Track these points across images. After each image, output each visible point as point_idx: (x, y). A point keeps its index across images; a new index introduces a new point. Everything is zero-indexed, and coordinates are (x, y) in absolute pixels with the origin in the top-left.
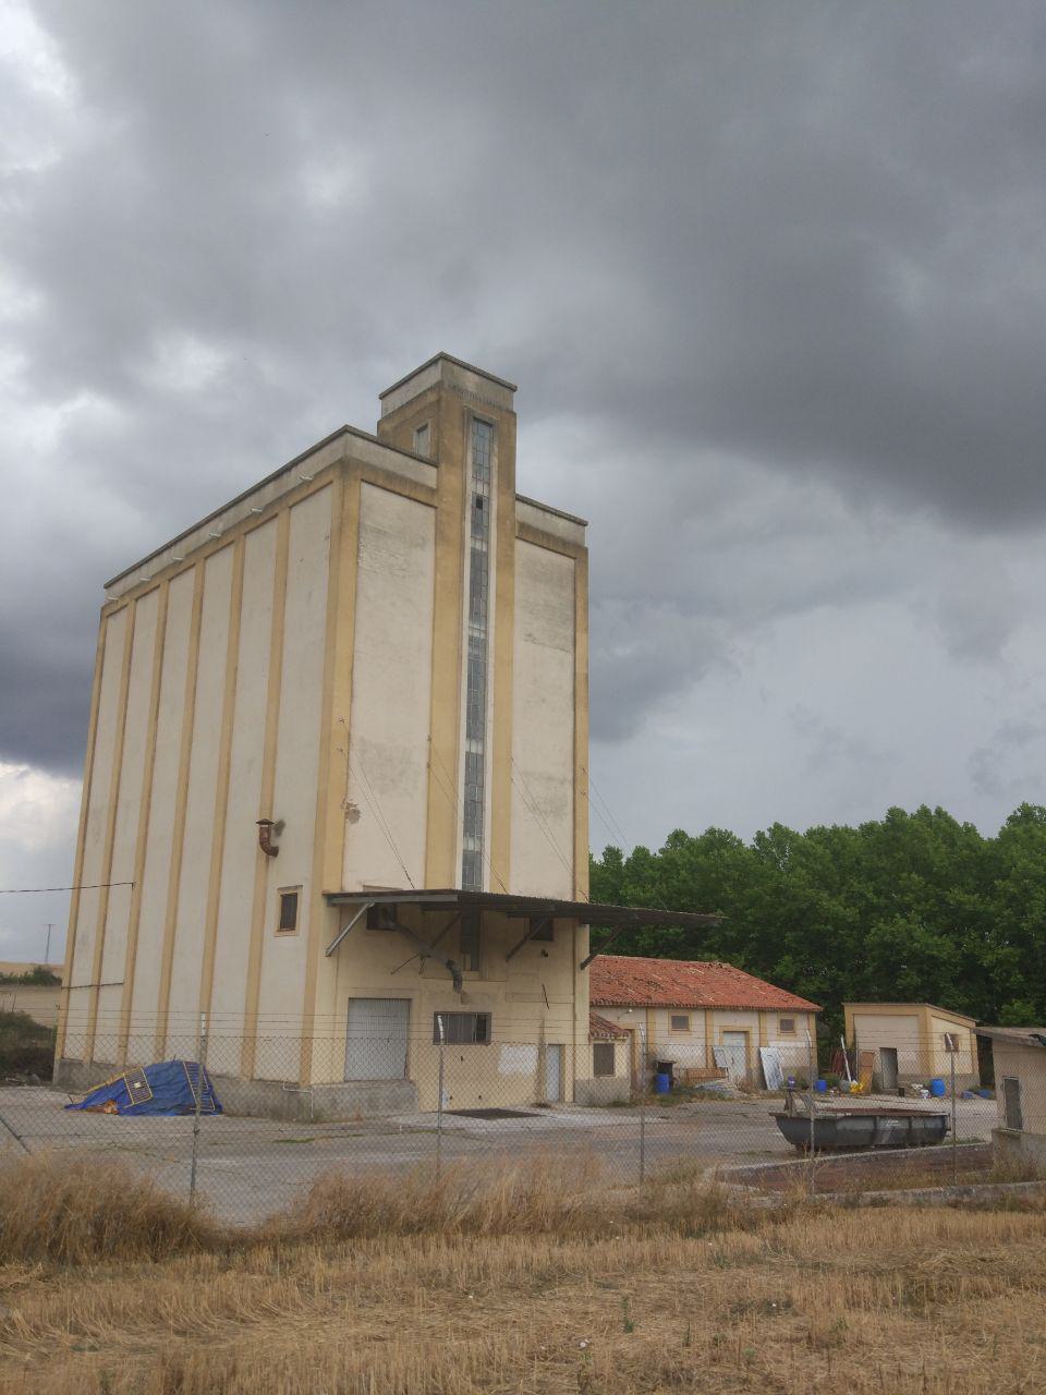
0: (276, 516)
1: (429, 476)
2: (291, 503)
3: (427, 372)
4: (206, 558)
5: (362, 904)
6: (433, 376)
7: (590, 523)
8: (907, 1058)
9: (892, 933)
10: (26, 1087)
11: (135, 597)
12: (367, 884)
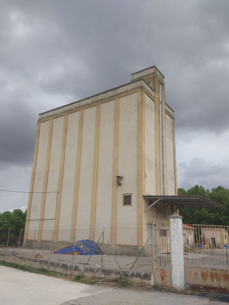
0: (114, 99)
1: (153, 93)
2: (120, 96)
3: (149, 70)
4: (84, 109)
5: (158, 199)
6: (152, 71)
7: (175, 112)
8: (218, 240)
9: (202, 212)
10: (4, 248)
11: (53, 118)
12: (148, 194)
